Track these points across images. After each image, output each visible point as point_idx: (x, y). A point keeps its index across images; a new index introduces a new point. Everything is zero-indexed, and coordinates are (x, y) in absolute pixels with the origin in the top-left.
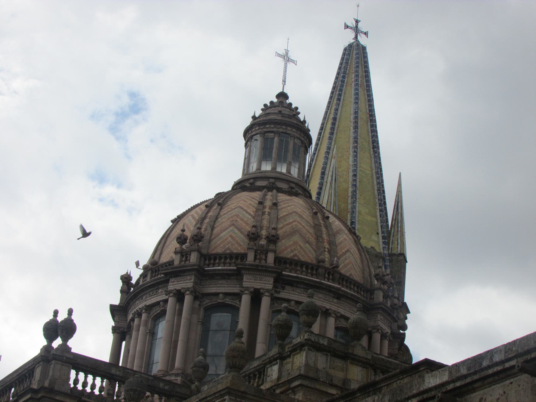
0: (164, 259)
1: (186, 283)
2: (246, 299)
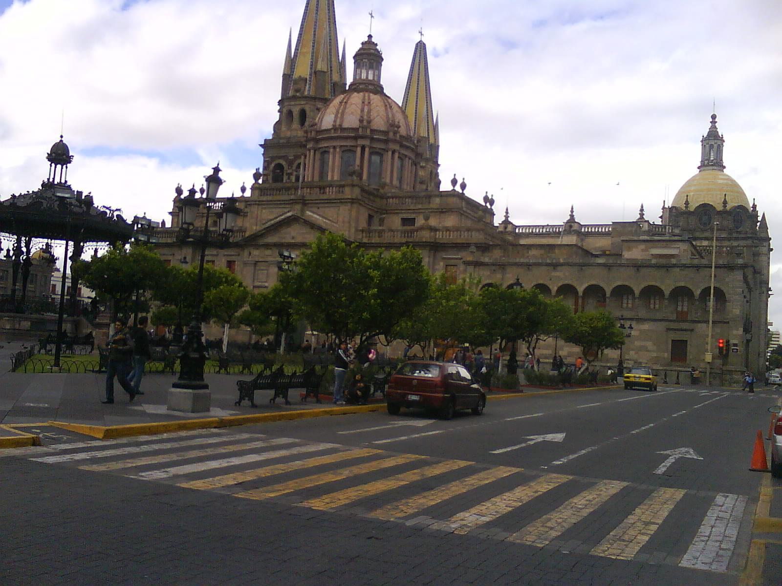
0: (345, 125)
1: (366, 142)
2: (390, 153)
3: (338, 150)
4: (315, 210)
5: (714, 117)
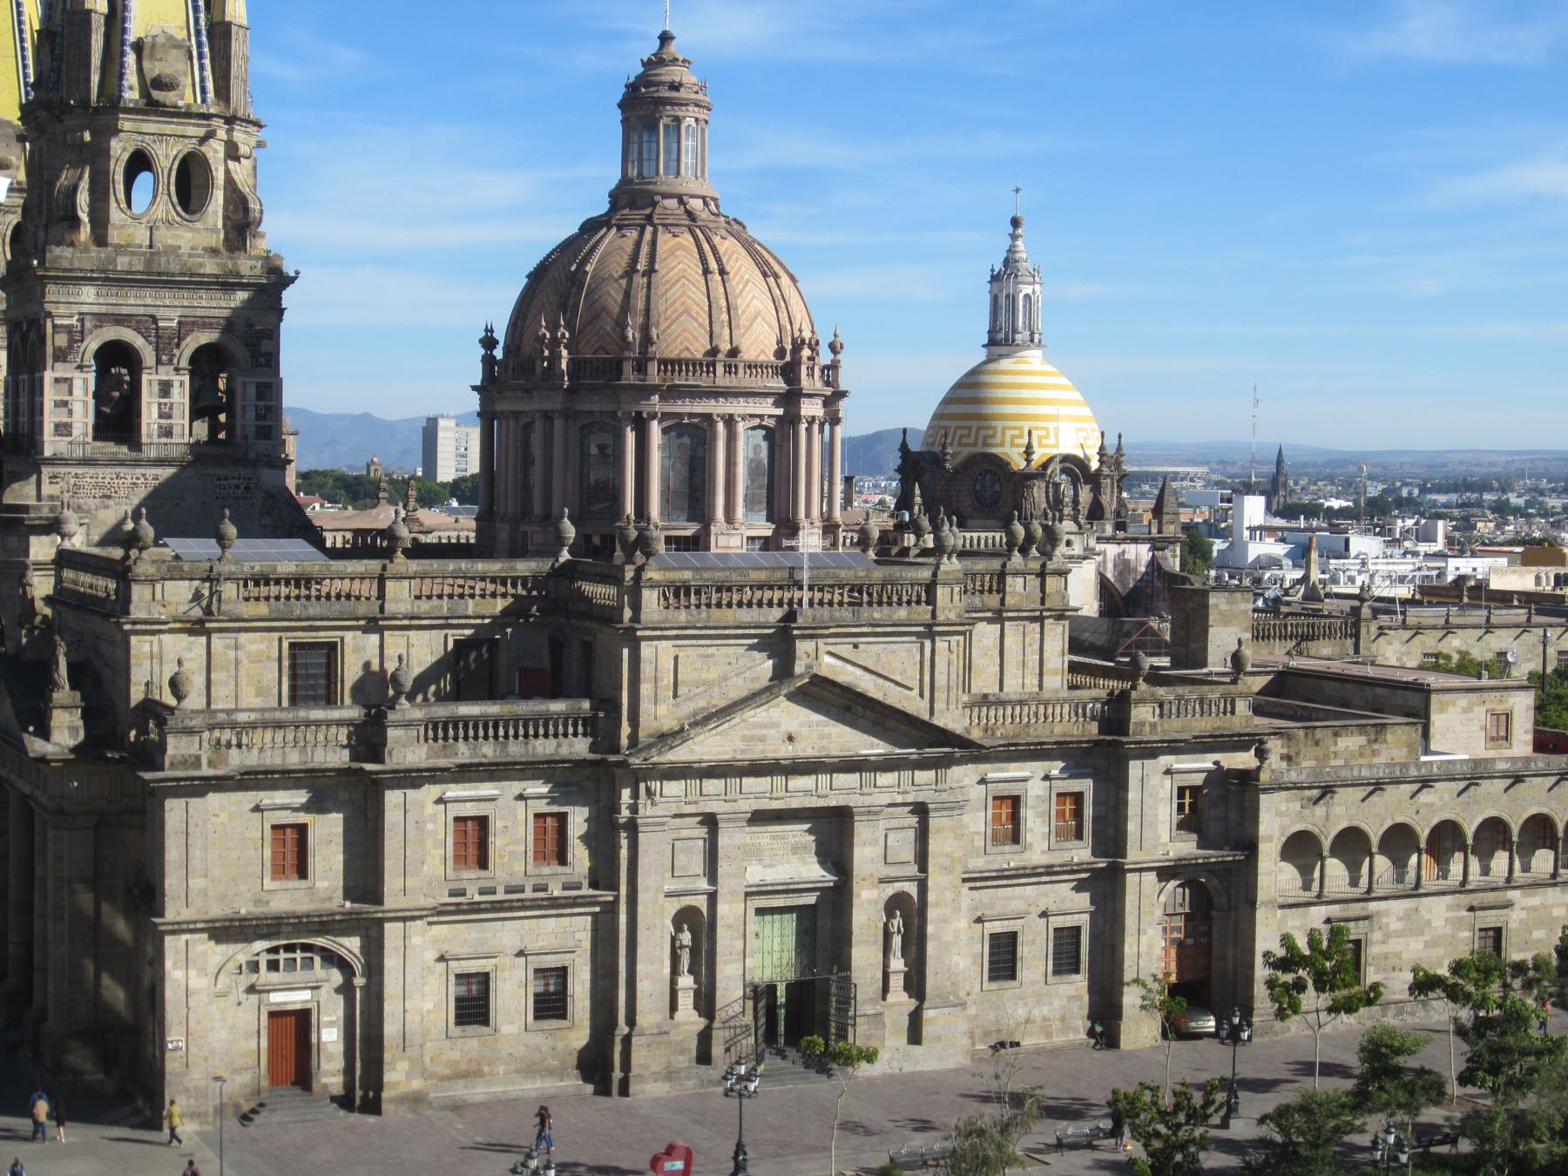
3: (741, 427)
4: (845, 649)
5: (1015, 223)
